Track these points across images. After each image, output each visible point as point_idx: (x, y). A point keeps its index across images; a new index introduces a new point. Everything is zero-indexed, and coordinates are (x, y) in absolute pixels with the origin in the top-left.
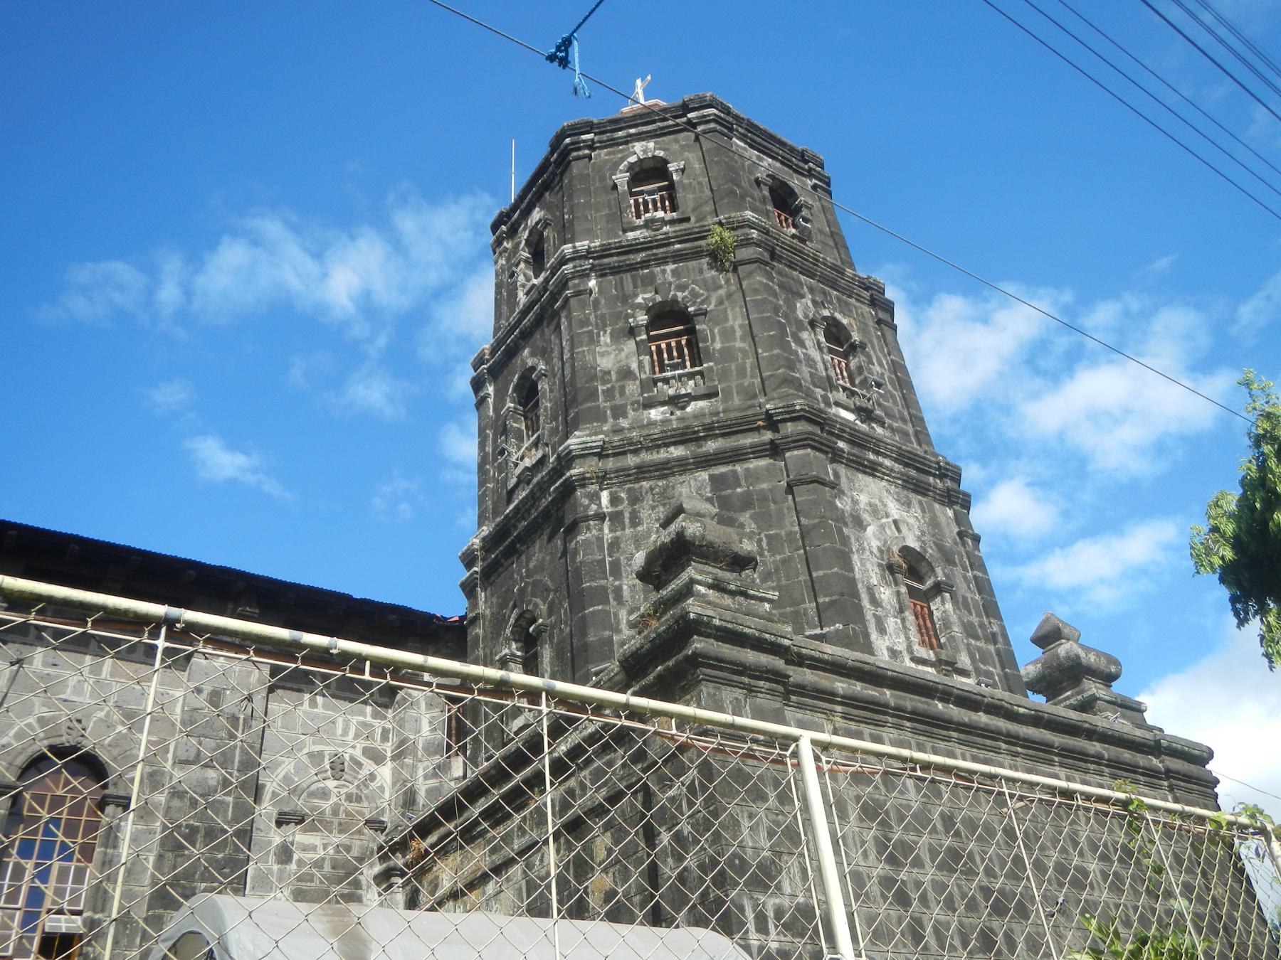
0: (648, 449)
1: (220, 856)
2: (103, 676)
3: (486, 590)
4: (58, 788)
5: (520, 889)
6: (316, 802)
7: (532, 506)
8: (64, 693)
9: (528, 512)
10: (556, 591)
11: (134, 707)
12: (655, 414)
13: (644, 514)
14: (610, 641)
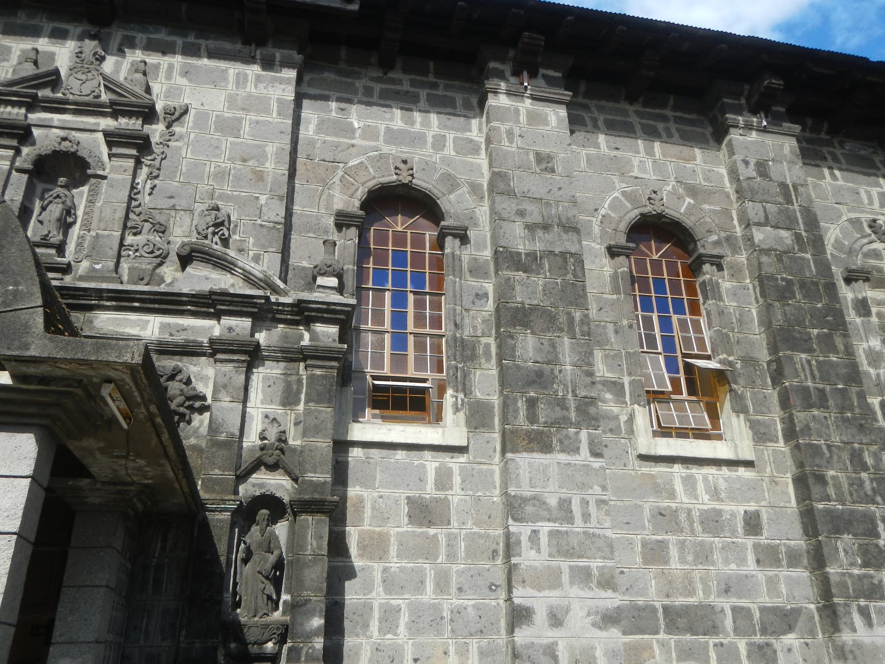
1: (819, 305)
2: (657, 157)
4: (652, 252)
6: (873, 262)
8: (633, 171)
11: (692, 182)
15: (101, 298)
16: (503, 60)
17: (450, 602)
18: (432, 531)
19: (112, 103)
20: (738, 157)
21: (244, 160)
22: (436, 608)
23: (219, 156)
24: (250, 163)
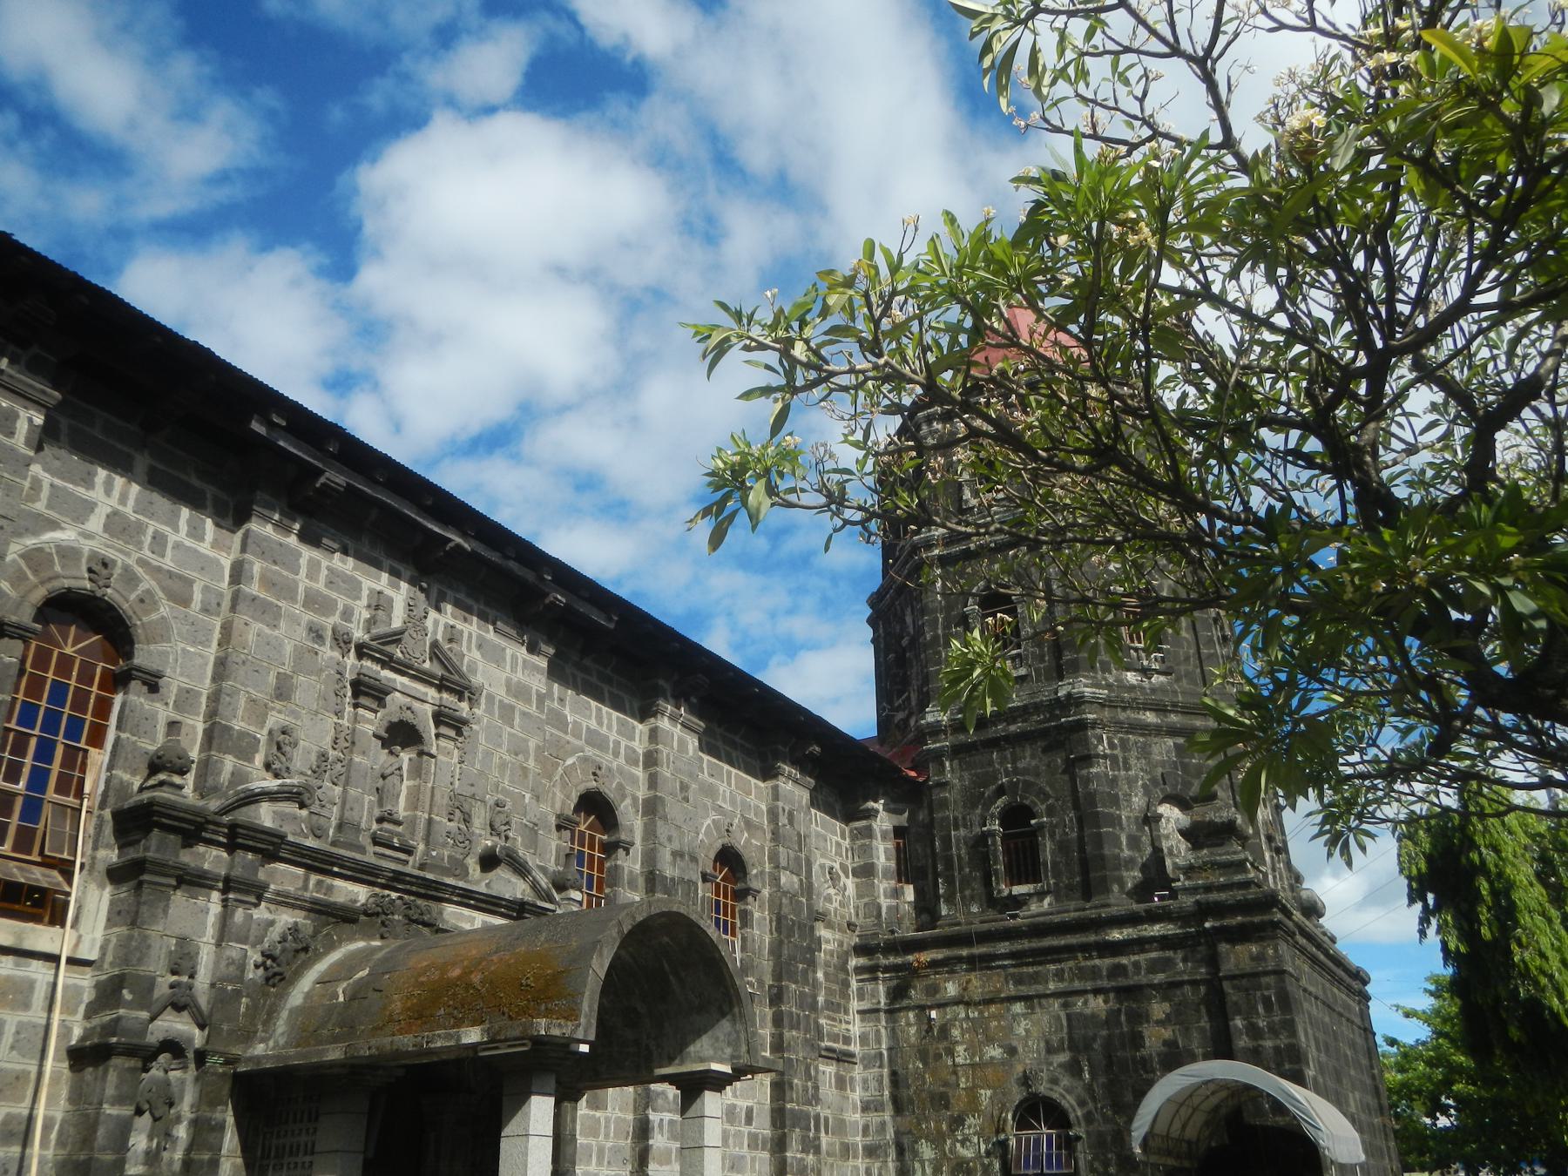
0: (1132, 708)
3: (951, 761)
5: (1059, 1018)
7: (1020, 716)
9: (1014, 721)
10: (1057, 800)
12: (1132, 677)
13: (1133, 761)
14: (1117, 857)
15: (452, 894)
18: (598, 1114)
19: (443, 678)
20: (780, 804)
21: (516, 755)
24: (520, 757)
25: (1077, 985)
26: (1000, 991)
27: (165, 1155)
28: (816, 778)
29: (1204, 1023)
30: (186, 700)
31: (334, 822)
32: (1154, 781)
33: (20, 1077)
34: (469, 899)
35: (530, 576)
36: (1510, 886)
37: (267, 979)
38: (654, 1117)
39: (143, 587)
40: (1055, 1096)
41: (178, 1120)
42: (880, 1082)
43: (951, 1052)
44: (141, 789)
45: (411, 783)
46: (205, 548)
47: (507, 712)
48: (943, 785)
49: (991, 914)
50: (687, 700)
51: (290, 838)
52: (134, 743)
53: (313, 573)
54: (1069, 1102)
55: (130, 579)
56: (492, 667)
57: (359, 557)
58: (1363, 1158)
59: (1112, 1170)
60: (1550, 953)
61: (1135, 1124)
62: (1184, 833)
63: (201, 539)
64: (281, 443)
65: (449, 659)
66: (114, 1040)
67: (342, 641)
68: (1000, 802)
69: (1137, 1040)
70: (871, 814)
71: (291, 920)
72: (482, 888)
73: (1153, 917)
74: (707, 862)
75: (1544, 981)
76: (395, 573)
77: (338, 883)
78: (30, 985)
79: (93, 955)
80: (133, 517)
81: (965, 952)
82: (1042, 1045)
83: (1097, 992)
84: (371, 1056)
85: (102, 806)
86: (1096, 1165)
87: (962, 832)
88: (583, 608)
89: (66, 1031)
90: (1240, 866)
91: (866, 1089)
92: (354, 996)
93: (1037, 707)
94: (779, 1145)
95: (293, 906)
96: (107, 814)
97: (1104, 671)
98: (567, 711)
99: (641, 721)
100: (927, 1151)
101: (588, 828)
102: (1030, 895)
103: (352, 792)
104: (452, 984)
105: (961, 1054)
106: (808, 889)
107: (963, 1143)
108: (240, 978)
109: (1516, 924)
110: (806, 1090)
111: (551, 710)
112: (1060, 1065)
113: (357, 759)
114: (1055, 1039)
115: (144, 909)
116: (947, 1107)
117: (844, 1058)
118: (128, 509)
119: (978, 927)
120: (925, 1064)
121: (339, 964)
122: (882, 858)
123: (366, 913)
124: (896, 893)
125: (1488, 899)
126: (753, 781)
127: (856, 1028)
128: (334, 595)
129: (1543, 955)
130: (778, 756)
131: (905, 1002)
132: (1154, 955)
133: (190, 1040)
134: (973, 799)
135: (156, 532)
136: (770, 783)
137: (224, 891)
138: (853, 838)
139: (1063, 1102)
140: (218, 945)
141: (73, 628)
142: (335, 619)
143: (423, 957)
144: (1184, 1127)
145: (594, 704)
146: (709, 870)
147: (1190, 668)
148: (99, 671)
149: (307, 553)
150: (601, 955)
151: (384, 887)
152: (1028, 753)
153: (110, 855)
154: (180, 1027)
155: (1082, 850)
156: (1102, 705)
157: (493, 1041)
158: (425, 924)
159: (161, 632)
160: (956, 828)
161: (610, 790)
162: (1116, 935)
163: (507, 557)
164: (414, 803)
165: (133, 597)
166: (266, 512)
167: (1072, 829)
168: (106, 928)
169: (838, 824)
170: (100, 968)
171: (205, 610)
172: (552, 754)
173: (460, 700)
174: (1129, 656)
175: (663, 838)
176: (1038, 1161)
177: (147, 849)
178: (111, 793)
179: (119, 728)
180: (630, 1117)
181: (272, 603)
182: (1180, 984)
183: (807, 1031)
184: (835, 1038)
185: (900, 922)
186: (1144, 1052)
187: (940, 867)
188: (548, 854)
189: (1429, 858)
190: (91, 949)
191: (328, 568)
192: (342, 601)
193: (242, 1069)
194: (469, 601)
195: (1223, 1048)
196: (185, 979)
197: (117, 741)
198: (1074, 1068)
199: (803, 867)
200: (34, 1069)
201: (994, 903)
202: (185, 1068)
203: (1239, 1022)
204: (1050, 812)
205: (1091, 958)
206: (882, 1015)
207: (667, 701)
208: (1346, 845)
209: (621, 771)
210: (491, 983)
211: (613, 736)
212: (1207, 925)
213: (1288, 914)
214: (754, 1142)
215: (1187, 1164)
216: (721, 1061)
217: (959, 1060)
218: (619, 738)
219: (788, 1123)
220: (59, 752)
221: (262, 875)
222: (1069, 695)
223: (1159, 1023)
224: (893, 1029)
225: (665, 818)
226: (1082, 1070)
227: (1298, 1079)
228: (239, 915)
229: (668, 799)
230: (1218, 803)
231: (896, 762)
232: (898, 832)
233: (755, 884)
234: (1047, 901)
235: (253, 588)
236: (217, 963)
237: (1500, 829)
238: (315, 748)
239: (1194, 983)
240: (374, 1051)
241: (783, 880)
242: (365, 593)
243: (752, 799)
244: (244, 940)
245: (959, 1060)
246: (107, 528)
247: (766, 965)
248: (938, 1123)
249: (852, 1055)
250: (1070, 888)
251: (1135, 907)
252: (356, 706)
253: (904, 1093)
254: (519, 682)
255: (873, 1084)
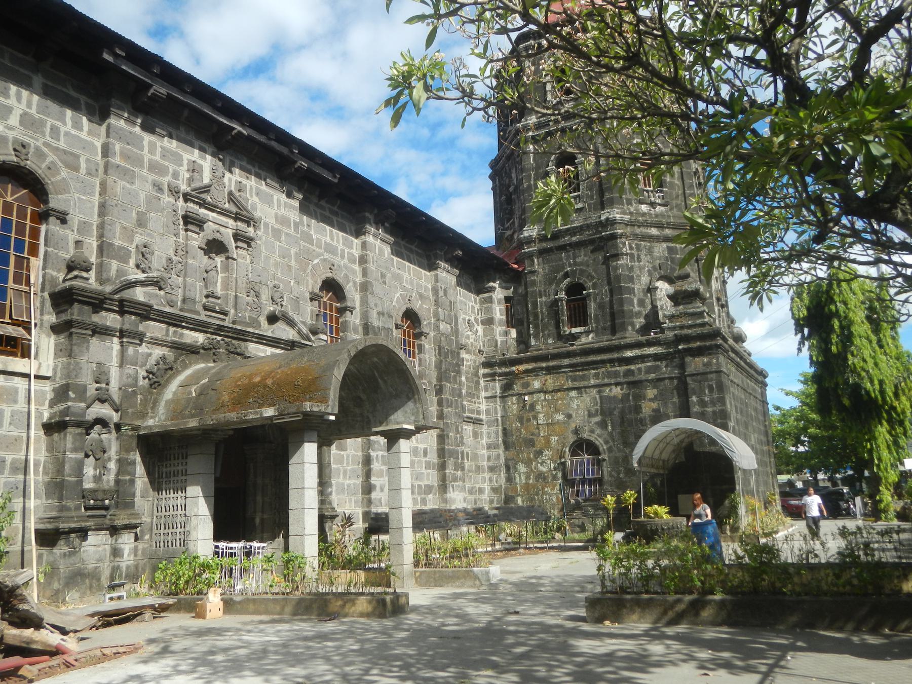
5: (595, 398)
9: (575, 235)
12: (644, 208)
13: (643, 257)
16: (371, 213)
17: (348, 482)
18: (342, 453)
19: (237, 213)
20: (439, 285)
22: (343, 484)
23: (274, 253)
24: (286, 260)
25: (606, 381)
26: (563, 385)
27: (104, 477)
28: (460, 270)
29: (676, 399)
30: (84, 227)
31: (180, 298)
32: (654, 268)
33: (17, 439)
34: (262, 339)
35: (284, 150)
36: (851, 323)
37: (151, 385)
38: (373, 453)
39: (49, 159)
40: (592, 439)
41: (109, 459)
42: (497, 434)
43: (536, 418)
44: (64, 281)
45: (223, 275)
46: (84, 135)
47: (277, 233)
48: (533, 272)
49: (560, 344)
50: (383, 225)
51: (155, 307)
52: (56, 254)
53: (152, 151)
54: (599, 442)
55: (41, 155)
56: (266, 207)
57: (180, 140)
58: (756, 466)
59: (621, 476)
60: (868, 359)
61: (635, 452)
62: (671, 297)
63: (80, 129)
64: (124, 67)
65: (239, 202)
66: (68, 418)
67: (174, 191)
68: (566, 282)
69: (638, 409)
70: (492, 290)
71: (161, 353)
72: (269, 334)
73: (650, 344)
74: (398, 318)
75: (863, 374)
76: (201, 149)
77: (186, 332)
78: (16, 391)
79: (49, 374)
80: (37, 116)
81: (544, 365)
82: (586, 413)
83: (617, 384)
84: (213, 424)
85: (43, 290)
86: (613, 473)
87: (544, 299)
88: (318, 170)
89: (40, 415)
90: (700, 315)
91: (489, 437)
92: (202, 393)
93: (588, 227)
94: (442, 467)
95: (162, 345)
96: (46, 295)
97: (628, 204)
98: (312, 232)
99: (357, 238)
100: (522, 468)
101: (329, 299)
102: (581, 333)
103: (189, 281)
104: (256, 385)
105: (541, 419)
106: (456, 332)
107: (542, 464)
108: (135, 385)
109: (852, 344)
110: (456, 438)
111: (303, 232)
112: (596, 423)
113: (190, 262)
114: (593, 410)
115: (75, 348)
116: (533, 446)
117: (477, 422)
118: (33, 111)
119: (552, 351)
120: (522, 424)
121: (191, 376)
122: (498, 315)
123: (203, 348)
124: (506, 334)
125: (838, 331)
126: (423, 272)
127: (483, 407)
128: (167, 164)
129: (864, 361)
130: (437, 257)
131: (511, 392)
132: (649, 364)
133: (111, 418)
134: (550, 280)
135: (52, 125)
136: (433, 273)
137: (121, 337)
138: (482, 303)
139: (596, 442)
140: (121, 367)
141: (10, 186)
142: (168, 178)
143: (237, 372)
144: (661, 453)
145: (328, 228)
146: (399, 322)
147: (679, 202)
148: (29, 211)
149: (147, 138)
150: (339, 368)
151: (213, 334)
152: (582, 253)
153: (51, 318)
154: (104, 411)
155: (612, 307)
156: (627, 225)
157: (281, 415)
158: (238, 354)
159: (64, 188)
160: (541, 297)
161: (340, 279)
162: (629, 354)
163: (270, 139)
164: (226, 286)
165: (43, 166)
166: (120, 112)
167: (606, 296)
168: (54, 359)
169: (473, 296)
170: (54, 380)
171: (89, 174)
172: (304, 258)
173: (249, 226)
174: (643, 195)
175: (372, 305)
176: (582, 472)
177: (72, 314)
178: (47, 283)
179: (46, 245)
180: (360, 454)
181: (129, 169)
182: (663, 379)
183: (456, 408)
184: (472, 412)
185: (508, 350)
186: (642, 415)
187: (531, 319)
188: (306, 314)
189: (808, 309)
190: (48, 371)
191: (161, 147)
192: (172, 167)
193: (142, 432)
194: (249, 167)
195: (685, 411)
196: (104, 385)
197: (46, 252)
198: (603, 425)
199: (453, 320)
200: (25, 435)
201: (560, 337)
202: (110, 433)
203: (694, 399)
204: (594, 286)
205: (614, 366)
206: (498, 399)
207: (371, 226)
208: (761, 299)
209: (346, 267)
210: (278, 384)
211: (340, 247)
212: (680, 347)
213: (725, 340)
214: (428, 466)
215: (661, 472)
216: (409, 424)
217: (540, 422)
218: (344, 248)
219: (447, 455)
220: (12, 260)
221: (141, 328)
222: (607, 219)
223: (651, 400)
224: (504, 406)
225: (373, 294)
226: (607, 426)
227: (725, 427)
228: (131, 350)
229: (374, 282)
230: (690, 280)
231: (506, 260)
232: (507, 299)
233: (425, 330)
234: (591, 336)
235: (117, 160)
236: (121, 377)
237: (849, 292)
238: (165, 256)
239: (671, 378)
240: (214, 421)
241: (442, 327)
242: (185, 162)
243: (423, 282)
244: (135, 364)
245: (540, 422)
246: (22, 123)
247: (433, 374)
248: (528, 454)
249: (482, 420)
250: (604, 329)
251: (640, 338)
252: (186, 230)
253: (510, 439)
254: (283, 215)
255: (493, 435)
